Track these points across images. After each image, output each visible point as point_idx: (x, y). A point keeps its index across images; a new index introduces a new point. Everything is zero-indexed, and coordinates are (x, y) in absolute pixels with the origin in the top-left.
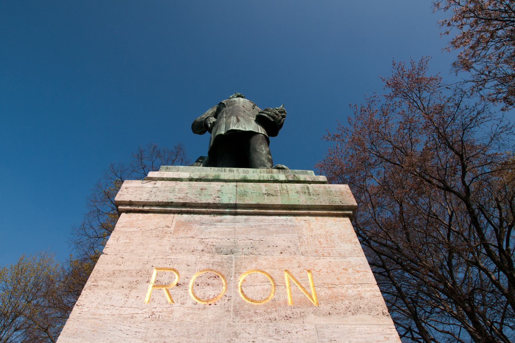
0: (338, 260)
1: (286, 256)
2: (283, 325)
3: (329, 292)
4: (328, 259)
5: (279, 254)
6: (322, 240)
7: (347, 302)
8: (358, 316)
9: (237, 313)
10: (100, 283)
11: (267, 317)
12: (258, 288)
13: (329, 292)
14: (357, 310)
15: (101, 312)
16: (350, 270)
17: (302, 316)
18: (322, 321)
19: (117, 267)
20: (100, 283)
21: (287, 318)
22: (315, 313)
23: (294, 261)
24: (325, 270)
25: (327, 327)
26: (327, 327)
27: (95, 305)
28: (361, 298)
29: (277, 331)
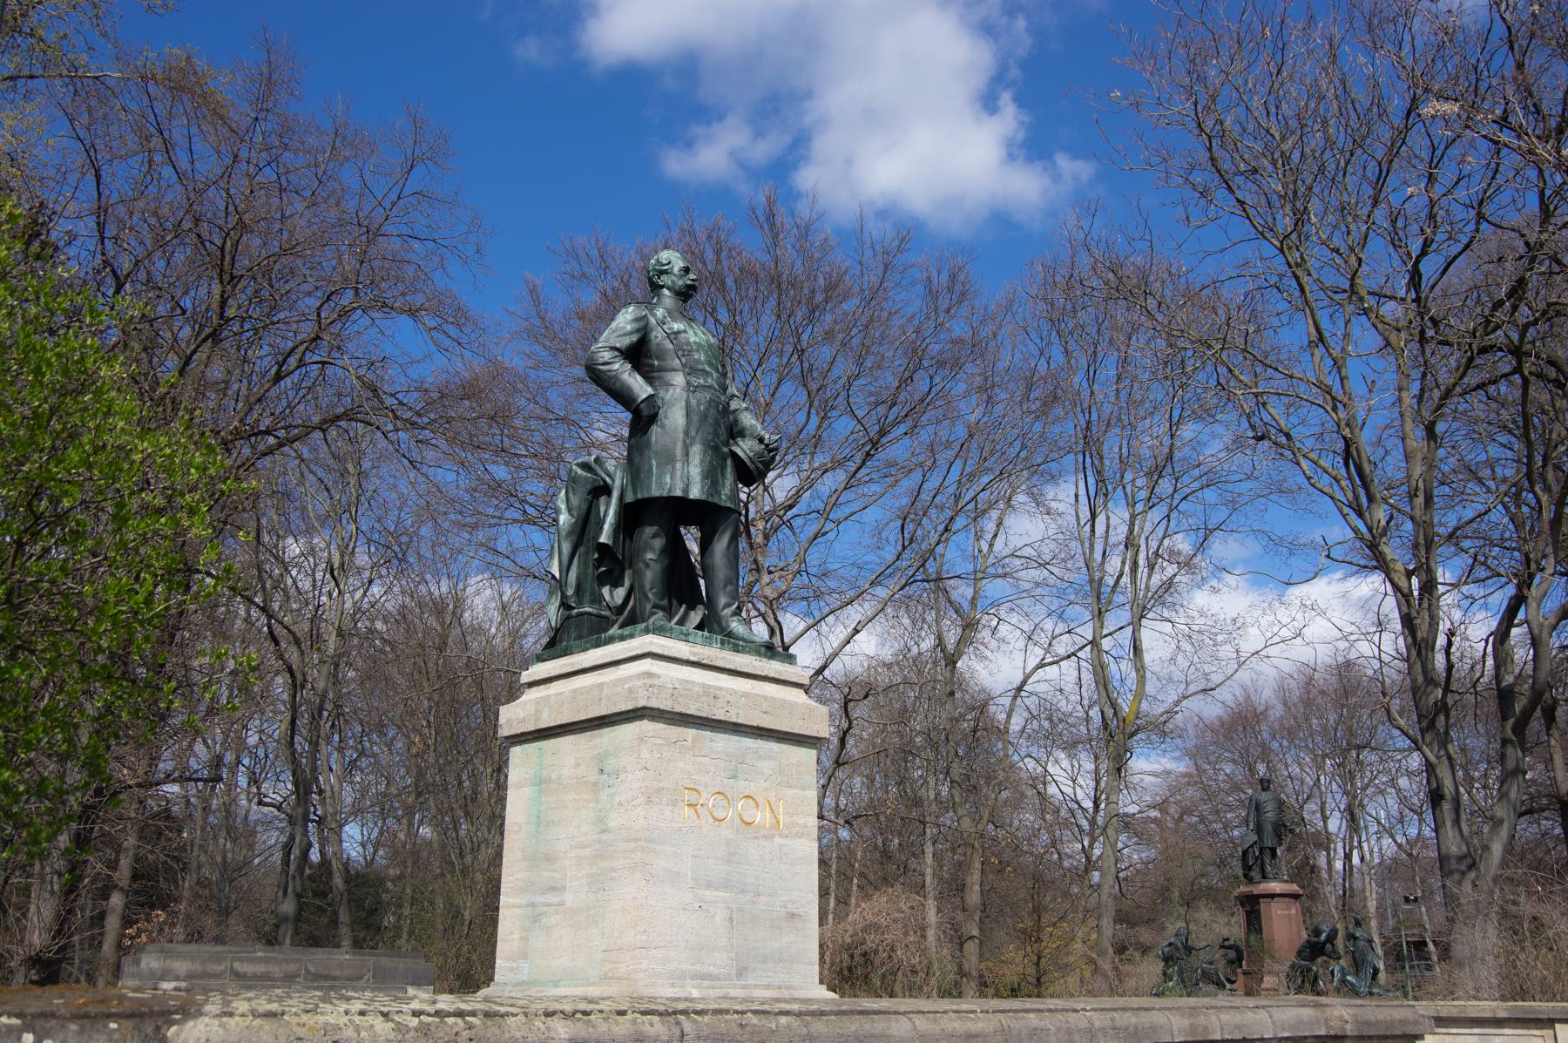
2: (762, 843)
17: (773, 836)
18: (783, 841)
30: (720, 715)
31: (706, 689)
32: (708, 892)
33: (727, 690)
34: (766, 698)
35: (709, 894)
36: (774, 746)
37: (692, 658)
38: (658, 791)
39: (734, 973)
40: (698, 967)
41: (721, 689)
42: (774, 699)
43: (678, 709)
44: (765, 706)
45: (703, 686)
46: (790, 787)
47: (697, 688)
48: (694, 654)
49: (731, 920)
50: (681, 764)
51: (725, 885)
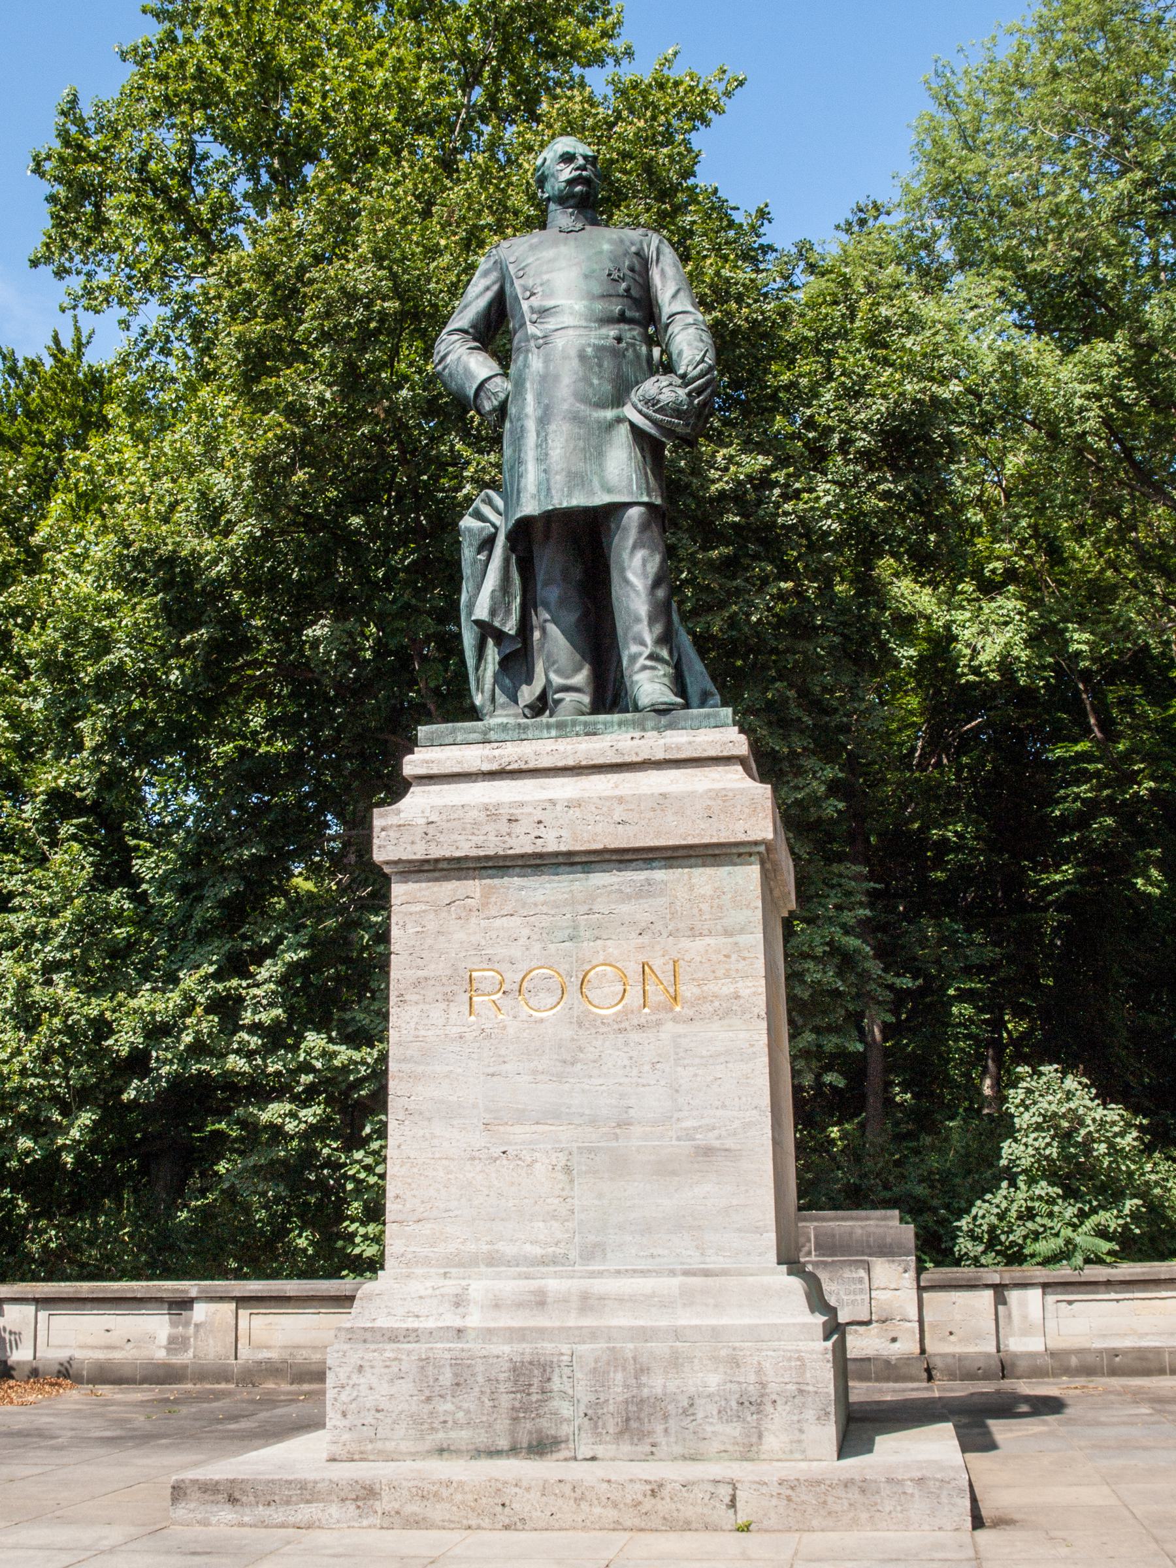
0: (722, 940)
1: (645, 939)
2: (635, 1036)
3: (696, 991)
4: (708, 940)
5: (634, 935)
6: (705, 907)
7: (717, 1004)
8: (726, 1022)
9: (580, 1024)
10: (407, 997)
11: (616, 1027)
12: (606, 990)
13: (696, 991)
15: (422, 1033)
16: (734, 957)
17: (659, 1023)
18: (681, 1029)
19: (420, 973)
20: (407, 997)
22: (674, 1020)
23: (657, 947)
24: (698, 959)
25: (685, 1036)
26: (685, 1036)
27: (413, 1025)
28: (737, 997)
29: (626, 1044)
30: (522, 845)
31: (491, 812)
32: (518, 1129)
34: (621, 800)
35: (521, 1133)
37: (486, 767)
38: (417, 983)
39: (574, 1254)
43: (436, 853)
44: (618, 813)
46: (693, 933)
47: (474, 814)
49: (568, 1170)
51: (554, 1115)
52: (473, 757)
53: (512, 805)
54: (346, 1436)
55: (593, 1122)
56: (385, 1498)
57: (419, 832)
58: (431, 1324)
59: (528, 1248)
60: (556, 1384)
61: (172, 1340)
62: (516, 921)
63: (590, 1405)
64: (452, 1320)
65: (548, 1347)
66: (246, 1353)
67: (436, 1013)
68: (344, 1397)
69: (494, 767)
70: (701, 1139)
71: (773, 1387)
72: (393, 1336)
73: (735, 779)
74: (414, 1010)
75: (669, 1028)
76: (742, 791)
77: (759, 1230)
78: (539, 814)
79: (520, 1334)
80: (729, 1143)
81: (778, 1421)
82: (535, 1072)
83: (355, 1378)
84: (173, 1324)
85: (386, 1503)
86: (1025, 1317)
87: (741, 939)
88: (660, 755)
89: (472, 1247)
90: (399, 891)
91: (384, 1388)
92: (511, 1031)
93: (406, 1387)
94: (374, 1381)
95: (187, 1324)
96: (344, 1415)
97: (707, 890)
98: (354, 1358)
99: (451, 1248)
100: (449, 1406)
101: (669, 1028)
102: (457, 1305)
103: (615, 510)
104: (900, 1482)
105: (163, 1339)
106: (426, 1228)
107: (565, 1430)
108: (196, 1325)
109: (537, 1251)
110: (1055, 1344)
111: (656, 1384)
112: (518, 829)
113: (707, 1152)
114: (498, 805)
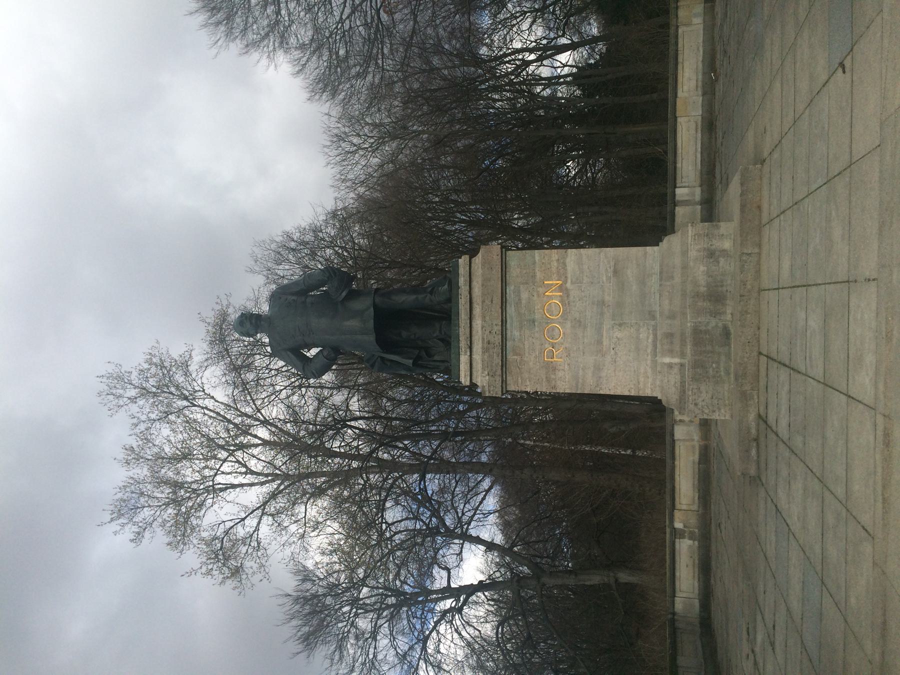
2: (571, 298)
14: (564, 264)
17: (567, 289)
18: (569, 281)
21: (568, 296)
31: (485, 350)
32: (605, 343)
33: (483, 334)
34: (483, 302)
35: (605, 342)
36: (510, 289)
39: (653, 323)
40: (649, 351)
41: (483, 339)
42: (483, 295)
44: (488, 302)
45: (483, 353)
46: (534, 276)
48: (466, 352)
49: (620, 325)
50: (531, 364)
51: (599, 330)
52: (464, 359)
53: (483, 343)
54: (723, 411)
55: (602, 314)
56: (746, 388)
57: (492, 379)
58: (678, 377)
59: (650, 340)
60: (703, 328)
61: (690, 538)
62: (526, 343)
63: (711, 316)
64: (676, 370)
65: (688, 332)
66: (695, 507)
67: (560, 374)
68: (707, 411)
69: (468, 350)
70: (610, 274)
71: (705, 246)
72: (683, 392)
73: (478, 260)
74: (558, 382)
75: (569, 285)
76: (483, 256)
77: (646, 253)
78: (487, 332)
79: (683, 342)
80: (612, 264)
81: (718, 244)
82: (583, 337)
83: (700, 407)
84: (684, 538)
85: (747, 387)
86: (688, 195)
87: (537, 258)
88: (468, 287)
89: (649, 362)
90: (512, 387)
91: (704, 395)
92: (567, 346)
93: (703, 388)
94: (700, 399)
95: (685, 531)
96: (714, 411)
97: (518, 270)
98: (692, 407)
99: (649, 370)
100: (711, 371)
101: (569, 285)
102: (671, 367)
103: (375, 306)
104: (742, 191)
105: (690, 542)
106: (642, 379)
107: (720, 325)
108: (685, 526)
109: (651, 337)
110: (698, 182)
111: (703, 289)
112: (492, 340)
113: (615, 272)
114: (483, 348)
